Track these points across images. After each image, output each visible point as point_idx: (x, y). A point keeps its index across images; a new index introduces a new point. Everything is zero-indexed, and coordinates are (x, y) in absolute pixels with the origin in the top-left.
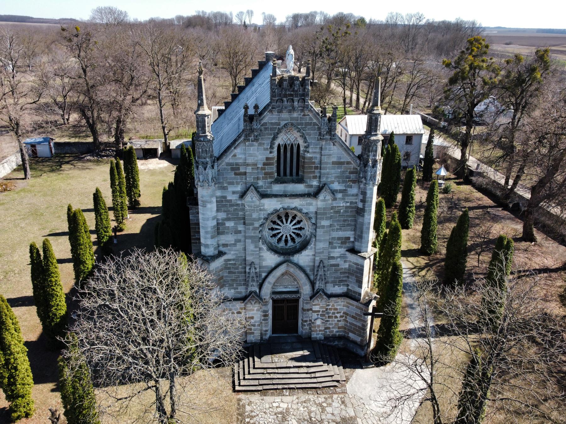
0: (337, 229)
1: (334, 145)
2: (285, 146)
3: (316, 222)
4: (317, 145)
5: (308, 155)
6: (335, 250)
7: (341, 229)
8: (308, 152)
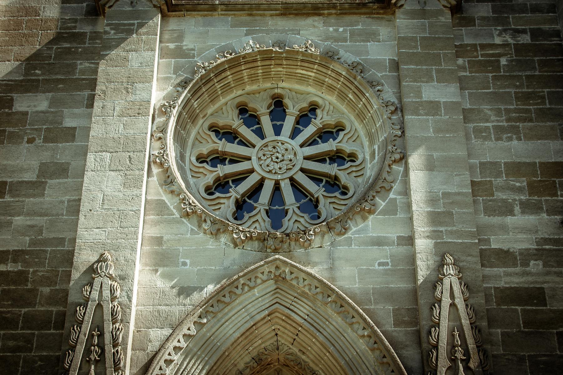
0: (499, 130)
3: (400, 99)
6: (509, 220)
7: (515, 130)
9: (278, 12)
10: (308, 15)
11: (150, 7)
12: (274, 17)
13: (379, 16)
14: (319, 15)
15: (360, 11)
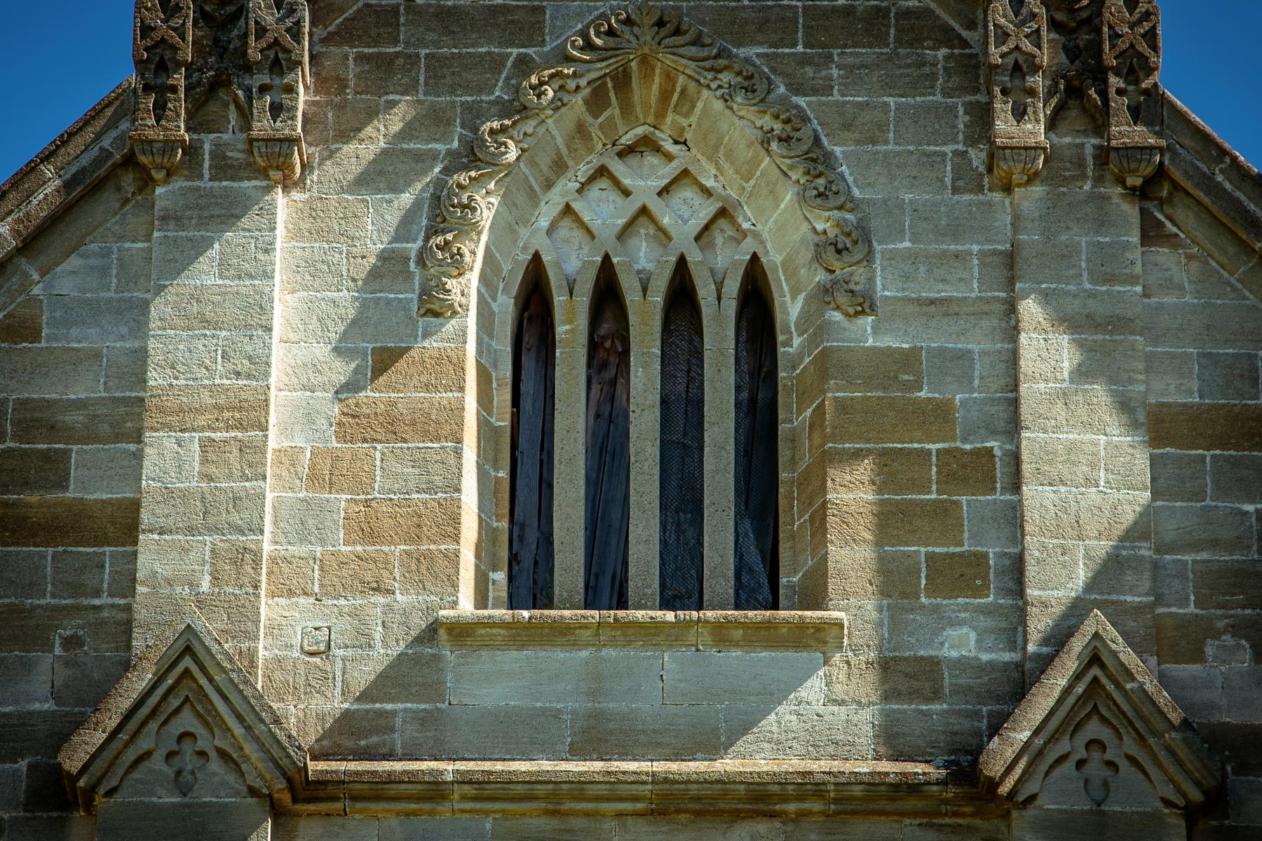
1: (1151, 233)
2: (607, 293)
4: (956, 232)
5: (866, 334)
8: (864, 304)
9: (640, 806)
10: (736, 816)
11: (237, 794)
12: (630, 820)
13: (960, 821)
14: (772, 815)
15: (899, 805)
